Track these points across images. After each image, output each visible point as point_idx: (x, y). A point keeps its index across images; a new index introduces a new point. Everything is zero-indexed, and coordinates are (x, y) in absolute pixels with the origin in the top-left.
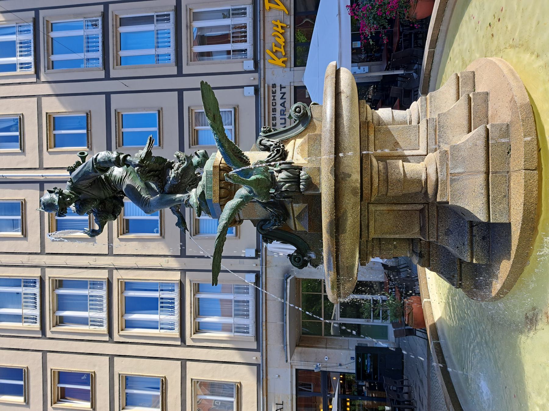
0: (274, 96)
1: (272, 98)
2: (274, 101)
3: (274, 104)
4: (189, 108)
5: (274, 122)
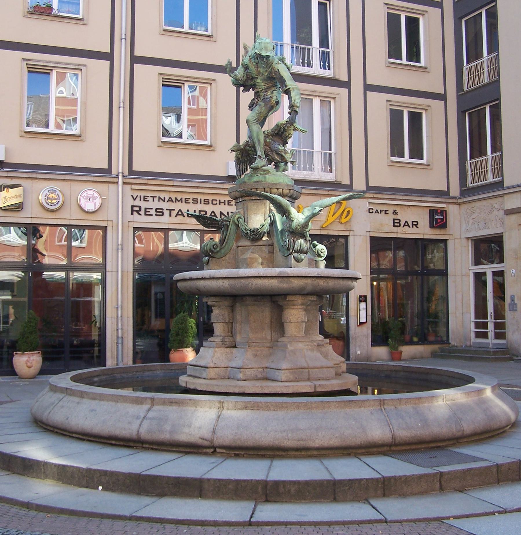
0: (224, 202)
1: (222, 201)
2: (218, 202)
3: (214, 202)
4: (214, 80)
5: (191, 201)
